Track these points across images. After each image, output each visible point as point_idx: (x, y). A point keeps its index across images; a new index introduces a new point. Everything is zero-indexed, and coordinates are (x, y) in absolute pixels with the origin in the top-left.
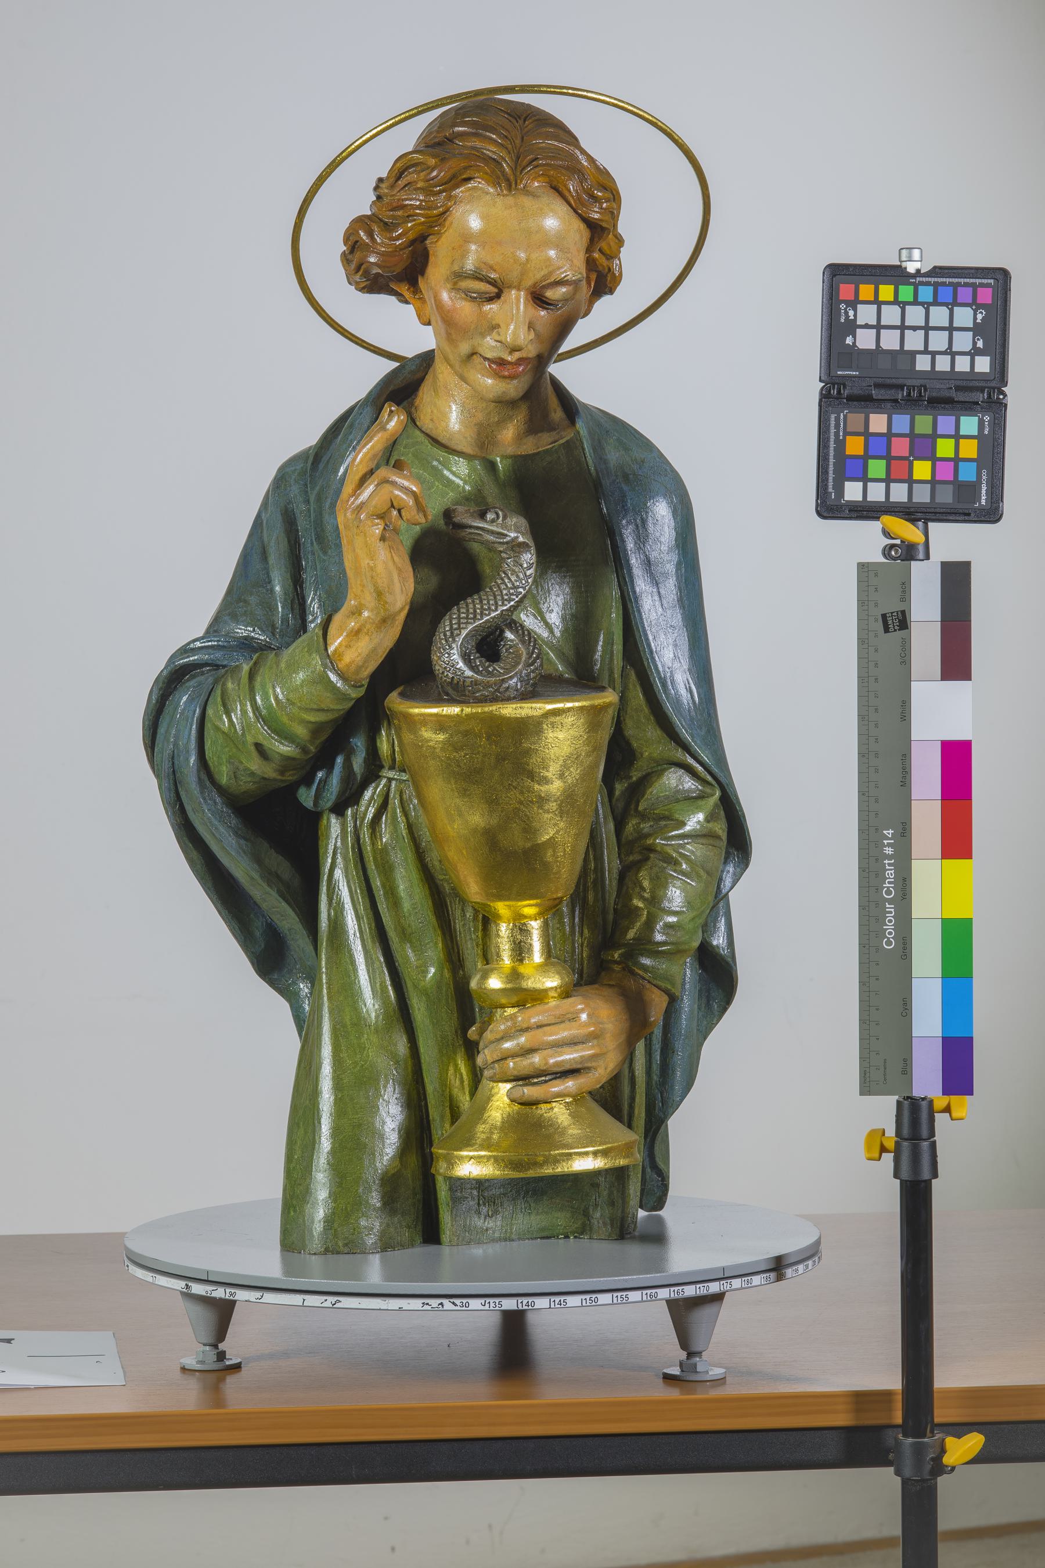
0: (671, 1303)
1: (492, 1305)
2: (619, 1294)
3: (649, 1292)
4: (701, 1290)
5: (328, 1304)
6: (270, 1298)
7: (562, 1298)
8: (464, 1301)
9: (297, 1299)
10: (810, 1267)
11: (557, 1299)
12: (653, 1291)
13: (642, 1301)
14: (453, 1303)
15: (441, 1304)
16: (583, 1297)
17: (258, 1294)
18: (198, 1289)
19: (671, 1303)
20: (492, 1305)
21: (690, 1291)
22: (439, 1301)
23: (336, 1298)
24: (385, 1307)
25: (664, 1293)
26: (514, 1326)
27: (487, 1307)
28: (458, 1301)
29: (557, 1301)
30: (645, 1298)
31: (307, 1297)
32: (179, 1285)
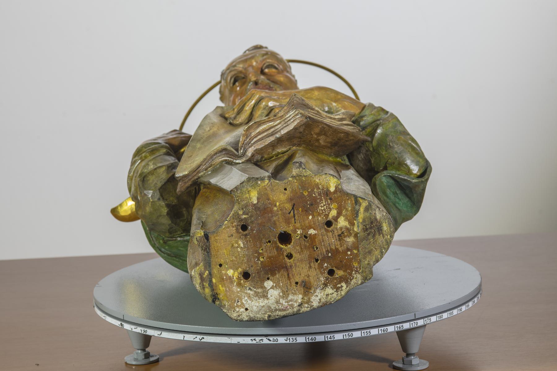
1: (291, 340)
2: (365, 331)
3: (382, 328)
4: (413, 325)
8: (275, 338)
10: (476, 302)
11: (329, 336)
12: (385, 328)
14: (269, 340)
15: (262, 340)
16: (344, 334)
17: (159, 332)
20: (291, 340)
21: (406, 326)
22: (261, 338)
27: (288, 342)
28: (271, 338)
29: (329, 336)
30: (380, 332)
32: (117, 323)
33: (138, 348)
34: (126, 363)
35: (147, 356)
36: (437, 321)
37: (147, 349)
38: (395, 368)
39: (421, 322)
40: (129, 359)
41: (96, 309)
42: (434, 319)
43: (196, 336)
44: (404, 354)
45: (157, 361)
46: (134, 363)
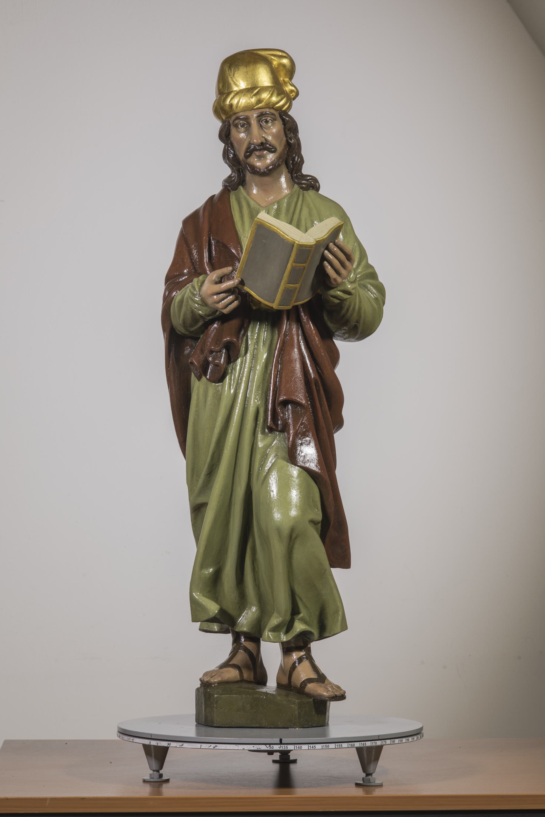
0: (359, 750)
5: (212, 747)
6: (186, 745)
7: (314, 745)
9: (198, 745)
13: (348, 747)
17: (181, 744)
18: (154, 743)
19: (359, 750)
21: (368, 744)
23: (214, 745)
24: (237, 748)
25: (357, 745)
26: (285, 761)
31: (202, 744)
33: (154, 769)
34: (144, 781)
35: (161, 776)
36: (390, 744)
37: (161, 772)
38: (357, 785)
39: (379, 743)
40: (147, 778)
41: (121, 735)
42: (388, 742)
43: (210, 745)
44: (364, 775)
45: (167, 781)
46: (152, 780)
